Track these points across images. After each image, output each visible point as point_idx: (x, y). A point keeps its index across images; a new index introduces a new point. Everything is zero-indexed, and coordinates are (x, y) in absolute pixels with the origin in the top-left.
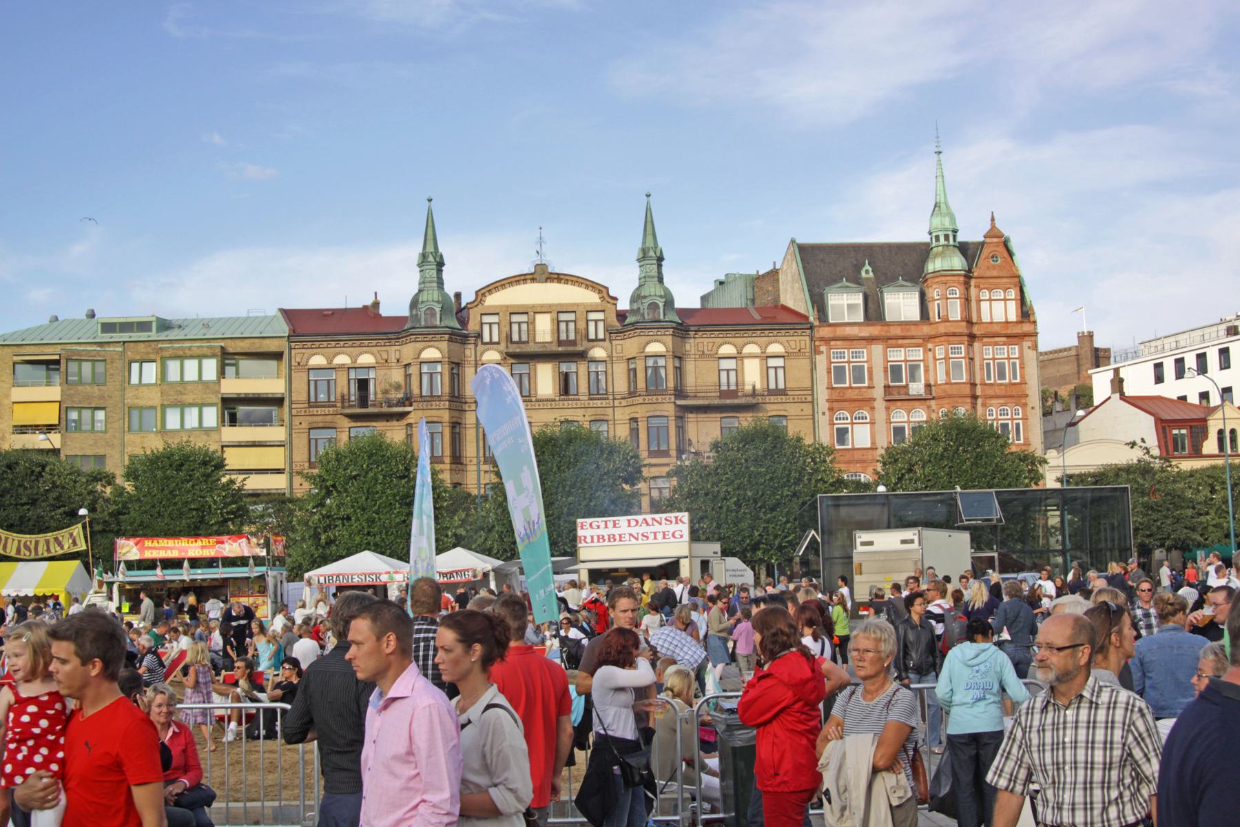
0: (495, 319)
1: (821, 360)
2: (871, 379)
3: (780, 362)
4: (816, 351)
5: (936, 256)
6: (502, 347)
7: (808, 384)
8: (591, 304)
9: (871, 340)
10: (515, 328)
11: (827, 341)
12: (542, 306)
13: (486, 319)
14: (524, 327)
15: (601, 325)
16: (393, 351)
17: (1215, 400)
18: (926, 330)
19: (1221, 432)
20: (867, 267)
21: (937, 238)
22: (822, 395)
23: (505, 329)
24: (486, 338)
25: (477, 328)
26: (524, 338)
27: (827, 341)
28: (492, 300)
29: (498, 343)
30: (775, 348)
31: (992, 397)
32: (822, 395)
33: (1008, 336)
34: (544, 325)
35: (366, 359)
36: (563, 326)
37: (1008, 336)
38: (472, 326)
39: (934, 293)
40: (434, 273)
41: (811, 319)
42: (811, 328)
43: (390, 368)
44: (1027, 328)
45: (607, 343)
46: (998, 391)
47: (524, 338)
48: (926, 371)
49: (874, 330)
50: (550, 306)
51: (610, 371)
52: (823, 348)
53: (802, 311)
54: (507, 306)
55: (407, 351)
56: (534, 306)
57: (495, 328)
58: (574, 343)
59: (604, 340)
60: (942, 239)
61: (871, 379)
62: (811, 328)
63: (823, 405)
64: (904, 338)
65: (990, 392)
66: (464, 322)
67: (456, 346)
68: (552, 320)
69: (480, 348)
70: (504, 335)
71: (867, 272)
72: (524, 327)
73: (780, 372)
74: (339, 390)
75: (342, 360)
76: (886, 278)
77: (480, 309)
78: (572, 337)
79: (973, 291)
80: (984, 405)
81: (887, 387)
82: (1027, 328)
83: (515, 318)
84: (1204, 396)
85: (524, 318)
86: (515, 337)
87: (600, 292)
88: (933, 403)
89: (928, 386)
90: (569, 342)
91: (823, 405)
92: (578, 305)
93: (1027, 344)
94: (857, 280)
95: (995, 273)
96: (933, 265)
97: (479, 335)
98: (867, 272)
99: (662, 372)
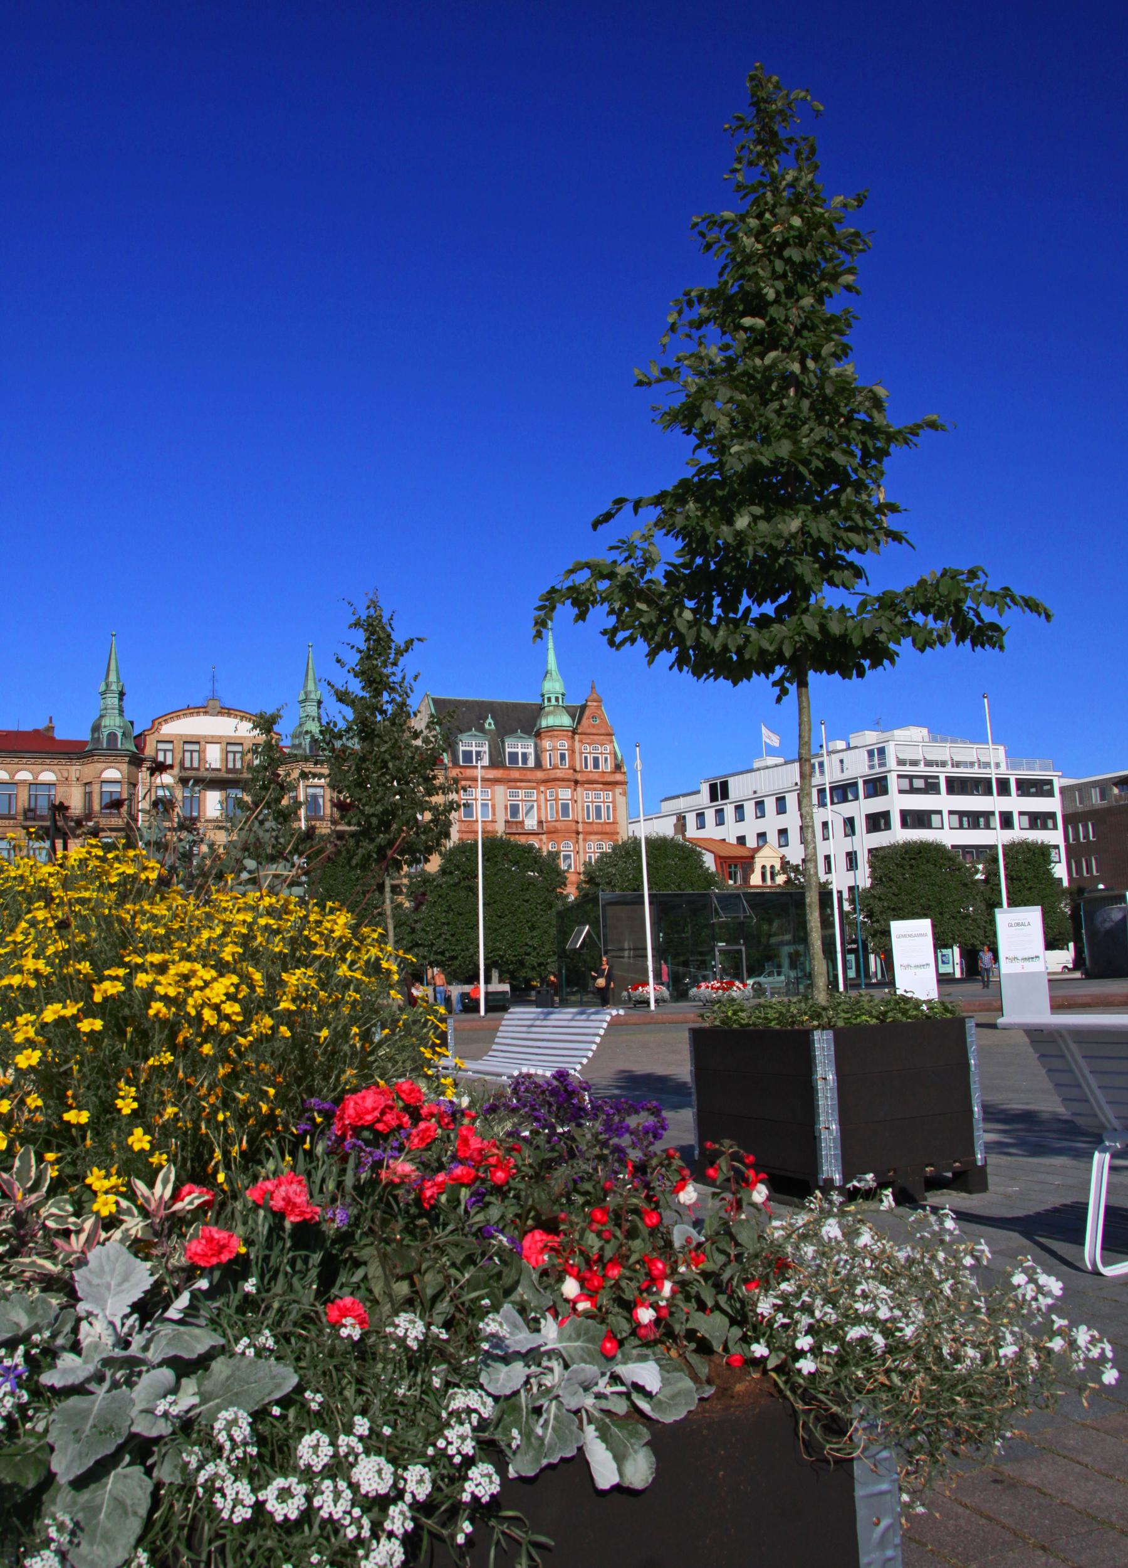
0: (169, 746)
5: (548, 714)
6: (176, 771)
9: (496, 781)
10: (188, 755)
13: (161, 746)
14: (196, 755)
16: (74, 770)
17: (751, 843)
18: (540, 775)
19: (764, 867)
20: (490, 720)
21: (549, 699)
23: (179, 757)
25: (153, 754)
26: (196, 765)
31: (591, 833)
33: (605, 783)
35: (47, 776)
36: (231, 756)
37: (605, 783)
38: (149, 751)
39: (547, 744)
40: (116, 701)
43: (70, 786)
44: (618, 777)
46: (595, 828)
47: (196, 765)
48: (539, 809)
55: (88, 770)
57: (169, 755)
58: (240, 771)
61: (494, 814)
64: (522, 781)
65: (588, 829)
66: (140, 747)
67: (133, 768)
70: (177, 761)
71: (489, 724)
72: (196, 755)
74: (20, 804)
75: (24, 775)
76: (505, 730)
77: (155, 737)
78: (238, 765)
79: (577, 744)
80: (585, 840)
81: (507, 822)
82: (618, 777)
83: (188, 747)
84: (741, 840)
85: (196, 747)
86: (187, 764)
88: (544, 837)
89: (540, 822)
90: (234, 770)
93: (618, 790)
94: (481, 729)
95: (594, 731)
96: (546, 722)
98: (489, 724)
99: (321, 801)
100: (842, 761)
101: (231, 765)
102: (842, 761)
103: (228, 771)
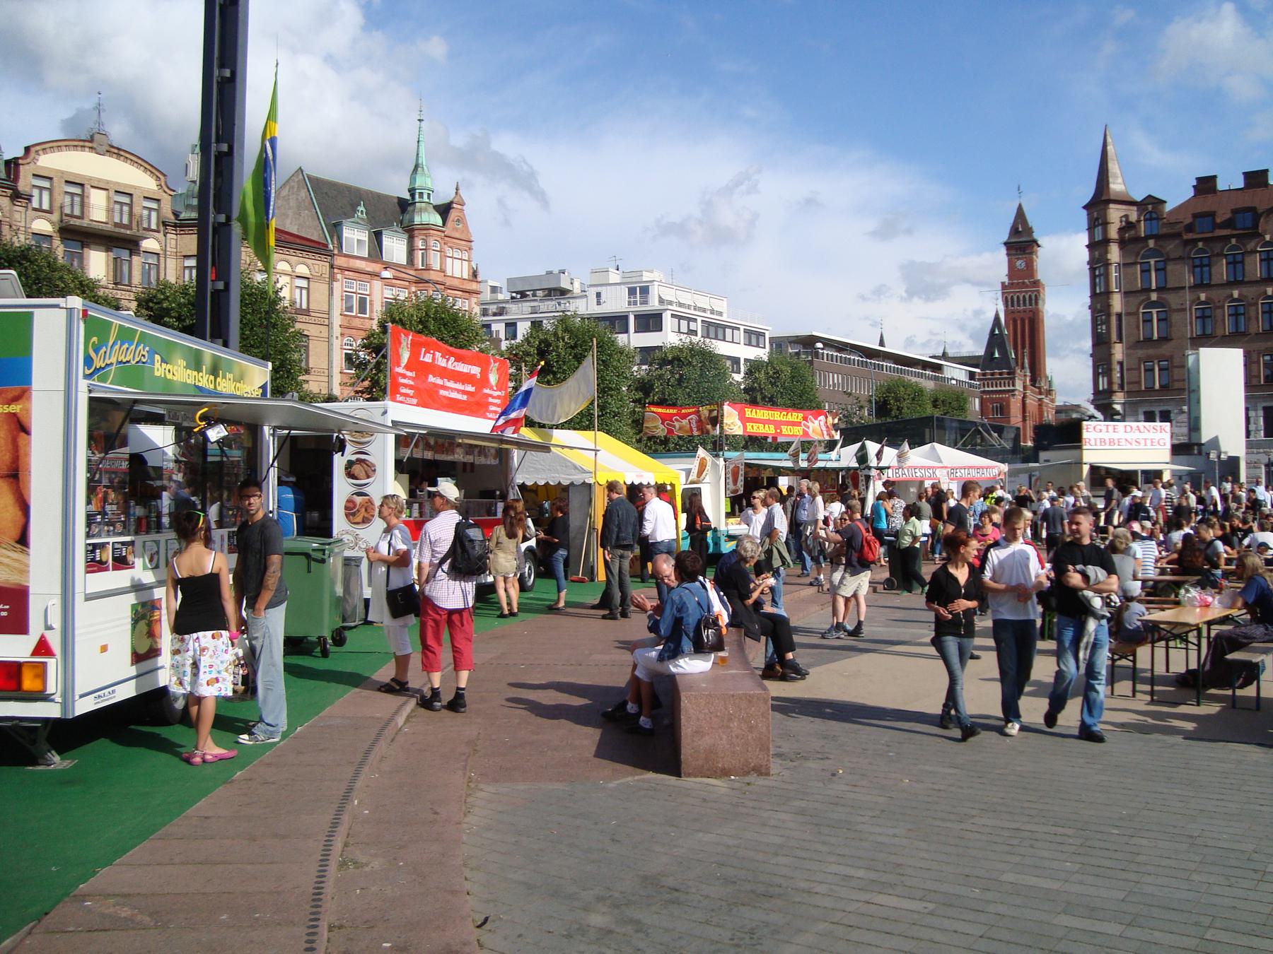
1: (337, 286)
2: (371, 311)
3: (304, 283)
4: (332, 278)
5: (421, 210)
7: (325, 308)
8: (148, 190)
11: (342, 269)
12: (99, 180)
15: (154, 215)
21: (421, 195)
22: (337, 320)
24: (35, 204)
27: (342, 269)
28: (47, 161)
29: (50, 212)
30: (302, 270)
32: (337, 320)
34: (98, 200)
41: (331, 246)
42: (332, 256)
44: (474, 286)
45: (160, 236)
49: (371, 267)
50: (108, 182)
51: (162, 266)
52: (339, 276)
53: (315, 238)
54: (63, 172)
56: (90, 179)
59: (158, 231)
60: (425, 196)
61: (371, 311)
62: (332, 256)
63: (337, 331)
68: (109, 198)
69: (30, 212)
73: (304, 292)
78: (125, 221)
87: (158, 179)
91: (337, 331)
92: (135, 188)
95: (457, 235)
97: (29, 198)
100: (598, 295)
101: (117, 220)
102: (598, 295)
103: (116, 225)
